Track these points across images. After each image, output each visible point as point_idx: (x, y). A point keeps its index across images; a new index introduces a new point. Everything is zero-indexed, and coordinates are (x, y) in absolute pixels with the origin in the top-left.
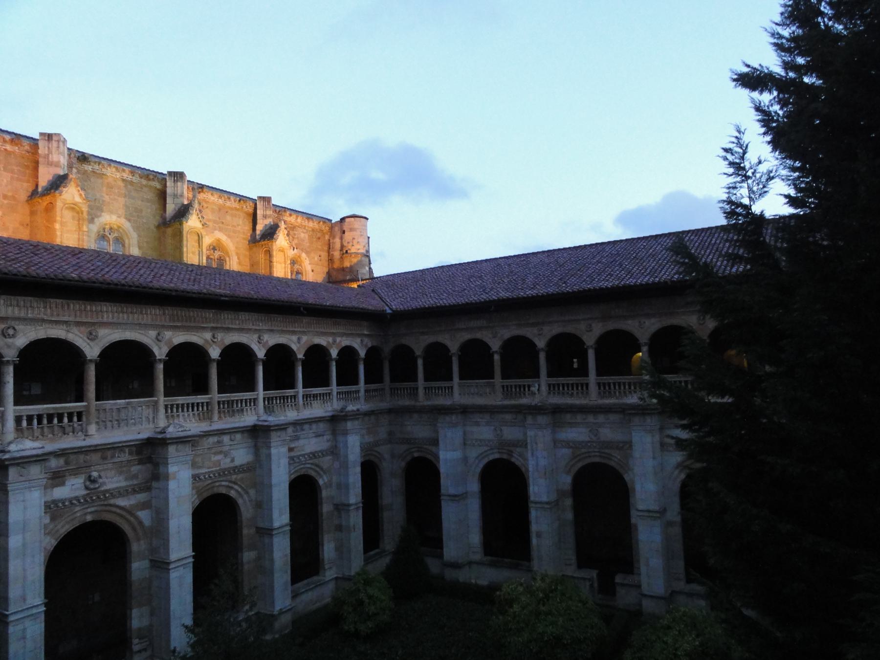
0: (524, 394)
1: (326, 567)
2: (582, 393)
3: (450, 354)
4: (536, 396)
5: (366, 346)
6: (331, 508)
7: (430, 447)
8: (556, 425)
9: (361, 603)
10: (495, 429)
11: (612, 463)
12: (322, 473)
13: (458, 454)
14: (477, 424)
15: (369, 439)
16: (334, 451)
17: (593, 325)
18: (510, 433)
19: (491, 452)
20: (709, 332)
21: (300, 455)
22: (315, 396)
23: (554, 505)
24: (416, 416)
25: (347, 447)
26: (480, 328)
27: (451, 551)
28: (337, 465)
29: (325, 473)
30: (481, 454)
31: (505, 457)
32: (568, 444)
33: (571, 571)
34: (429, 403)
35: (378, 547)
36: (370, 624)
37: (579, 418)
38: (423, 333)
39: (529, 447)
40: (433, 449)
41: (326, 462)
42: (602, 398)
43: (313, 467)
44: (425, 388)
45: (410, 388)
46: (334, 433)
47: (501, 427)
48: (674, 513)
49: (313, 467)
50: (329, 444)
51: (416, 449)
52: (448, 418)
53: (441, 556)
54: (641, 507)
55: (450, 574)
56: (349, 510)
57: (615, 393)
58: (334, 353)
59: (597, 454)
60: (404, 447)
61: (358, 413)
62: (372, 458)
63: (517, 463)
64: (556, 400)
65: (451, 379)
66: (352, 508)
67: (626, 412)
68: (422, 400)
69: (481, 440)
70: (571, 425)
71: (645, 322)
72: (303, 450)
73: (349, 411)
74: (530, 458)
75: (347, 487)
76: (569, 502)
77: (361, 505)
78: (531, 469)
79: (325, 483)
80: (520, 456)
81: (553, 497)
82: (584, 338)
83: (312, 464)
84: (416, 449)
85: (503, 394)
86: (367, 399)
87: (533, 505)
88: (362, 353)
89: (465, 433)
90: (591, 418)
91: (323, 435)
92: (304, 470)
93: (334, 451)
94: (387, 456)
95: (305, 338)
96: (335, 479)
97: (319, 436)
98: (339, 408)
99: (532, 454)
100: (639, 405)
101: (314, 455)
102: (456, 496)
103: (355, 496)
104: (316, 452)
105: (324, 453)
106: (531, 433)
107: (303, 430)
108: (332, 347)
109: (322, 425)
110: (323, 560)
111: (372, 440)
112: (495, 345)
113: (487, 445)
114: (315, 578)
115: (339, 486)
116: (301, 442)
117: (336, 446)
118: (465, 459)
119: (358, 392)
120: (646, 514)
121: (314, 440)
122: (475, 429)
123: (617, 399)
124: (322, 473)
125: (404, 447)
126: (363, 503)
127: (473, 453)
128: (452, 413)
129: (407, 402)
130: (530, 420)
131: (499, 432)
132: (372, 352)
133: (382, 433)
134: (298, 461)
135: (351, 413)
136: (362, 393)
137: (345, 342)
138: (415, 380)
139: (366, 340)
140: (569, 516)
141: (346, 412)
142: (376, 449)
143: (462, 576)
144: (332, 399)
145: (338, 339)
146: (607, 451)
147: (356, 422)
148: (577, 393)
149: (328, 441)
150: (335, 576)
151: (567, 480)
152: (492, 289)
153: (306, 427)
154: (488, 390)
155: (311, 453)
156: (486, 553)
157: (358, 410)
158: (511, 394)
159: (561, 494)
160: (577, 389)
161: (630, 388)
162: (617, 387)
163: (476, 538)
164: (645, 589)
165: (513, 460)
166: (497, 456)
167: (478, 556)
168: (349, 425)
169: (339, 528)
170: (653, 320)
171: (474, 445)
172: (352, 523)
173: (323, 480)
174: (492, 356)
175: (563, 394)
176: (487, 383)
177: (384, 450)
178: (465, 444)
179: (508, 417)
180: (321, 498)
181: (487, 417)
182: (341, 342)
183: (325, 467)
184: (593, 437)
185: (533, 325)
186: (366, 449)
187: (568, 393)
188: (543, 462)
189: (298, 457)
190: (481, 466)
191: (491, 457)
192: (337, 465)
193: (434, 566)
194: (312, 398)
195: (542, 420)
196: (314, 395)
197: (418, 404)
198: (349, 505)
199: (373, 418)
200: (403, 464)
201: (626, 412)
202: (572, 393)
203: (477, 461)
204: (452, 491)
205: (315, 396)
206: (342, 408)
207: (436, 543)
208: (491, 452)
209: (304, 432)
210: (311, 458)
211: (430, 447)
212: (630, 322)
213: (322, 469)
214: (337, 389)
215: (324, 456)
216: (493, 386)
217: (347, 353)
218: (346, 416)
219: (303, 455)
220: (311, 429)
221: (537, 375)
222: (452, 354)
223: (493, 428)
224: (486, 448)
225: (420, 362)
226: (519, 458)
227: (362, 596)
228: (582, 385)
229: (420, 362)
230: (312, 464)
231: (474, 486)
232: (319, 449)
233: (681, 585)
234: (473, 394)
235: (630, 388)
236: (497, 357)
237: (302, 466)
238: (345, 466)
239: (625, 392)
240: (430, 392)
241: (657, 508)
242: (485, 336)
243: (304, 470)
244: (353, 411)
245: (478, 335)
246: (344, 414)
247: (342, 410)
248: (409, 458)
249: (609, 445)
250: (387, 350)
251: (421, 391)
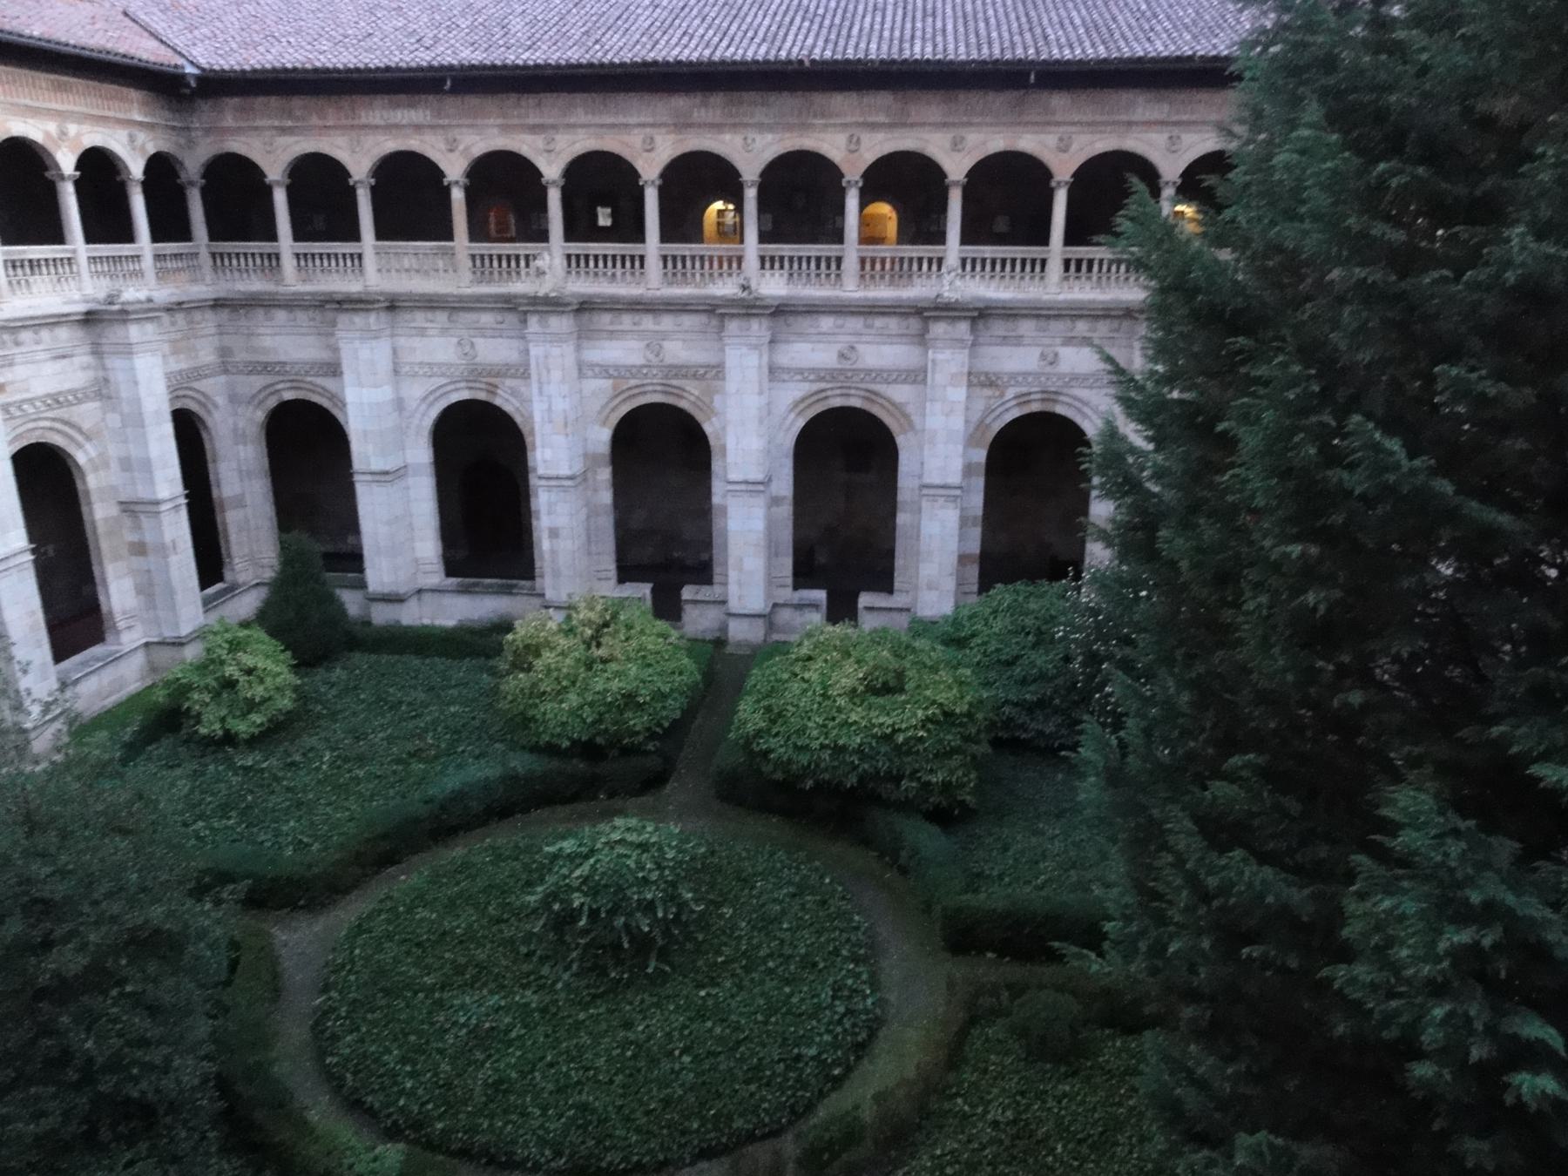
0: (518, 273)
1: (121, 625)
2: (633, 274)
3: (351, 183)
4: (547, 277)
5: (143, 148)
6: (114, 511)
7: (319, 381)
8: (584, 335)
9: (230, 684)
10: (459, 343)
11: (683, 404)
12: (79, 438)
13: (385, 393)
14: (422, 332)
15: (180, 364)
16: (102, 390)
17: (659, 139)
18: (495, 350)
19: (452, 387)
20: (863, 167)
21: (24, 401)
22: (34, 265)
23: (580, 480)
24: (281, 316)
25: (136, 383)
26: (418, 128)
27: (380, 572)
28: (114, 420)
29: (88, 438)
30: (431, 393)
31: (482, 396)
32: (605, 371)
33: (610, 589)
34: (308, 288)
35: (221, 579)
36: (257, 718)
37: (627, 320)
38: (283, 131)
39: (534, 376)
40: (329, 383)
41: (87, 414)
42: (670, 284)
43: (58, 426)
44: (297, 256)
45: (261, 255)
46: (97, 351)
47: (474, 340)
48: (784, 485)
49: (58, 426)
50: (91, 374)
51: (288, 385)
52: (358, 319)
53: (362, 585)
54: (733, 476)
55: (381, 615)
56: (159, 513)
57: (693, 275)
58: (67, 162)
59: (659, 388)
60: (258, 381)
61: (151, 305)
62: (193, 406)
63: (507, 408)
64: (582, 286)
65: (354, 235)
66: (163, 507)
67: (716, 311)
68: (292, 279)
69: (430, 365)
70: (612, 335)
71: (754, 140)
72: (27, 390)
73: (129, 303)
74: (536, 398)
75: (147, 465)
76: (605, 474)
77: (184, 501)
78: (537, 417)
79: (91, 460)
80: (512, 394)
81: (578, 468)
82: (640, 165)
83: (53, 420)
84: (288, 385)
85: (474, 273)
86: (162, 275)
87: (543, 482)
88: (136, 168)
89: (395, 351)
90: (648, 322)
91: (72, 356)
92: (38, 433)
93: (102, 390)
94: (220, 400)
96: (114, 451)
97: (64, 357)
98: (102, 295)
99: (541, 392)
100: (743, 300)
101: (56, 400)
102: (386, 473)
103: (168, 481)
104: (60, 393)
105: (80, 396)
106: (536, 351)
107: (17, 344)
108: (59, 147)
109: (63, 333)
110: (110, 613)
111: (184, 366)
112: (454, 169)
113: (443, 375)
114: (96, 650)
115: (126, 464)
116: (20, 372)
117: (106, 380)
118: (399, 404)
119: (137, 258)
120: (743, 487)
121: (50, 368)
122: (417, 342)
123: (697, 286)
124: (79, 438)
125: (258, 381)
126: (187, 496)
127: (415, 391)
128: (368, 310)
129: (255, 284)
130: (534, 323)
131: (467, 349)
132: (161, 169)
133: (207, 355)
134: (18, 413)
135: (138, 306)
136: (148, 262)
137: (94, 137)
138: (272, 236)
139: (142, 137)
140: (606, 497)
141: (123, 303)
142: (196, 385)
143: (412, 615)
144: (79, 273)
145: (72, 129)
146: (674, 382)
147: (150, 327)
148: (624, 274)
149: (85, 368)
150: (144, 641)
151: (602, 437)
152: (436, 40)
153: (26, 336)
154: (440, 264)
155: (48, 395)
156: (450, 571)
157: (150, 300)
158: (491, 273)
159: (591, 459)
160: (623, 266)
161: (721, 267)
162: (698, 265)
163: (428, 547)
164: (734, 605)
165: (498, 402)
166: (465, 395)
167: (435, 575)
168: (134, 332)
169: (139, 549)
170: (769, 137)
171: (415, 375)
172: (168, 538)
173: (85, 452)
174: (446, 191)
175: (596, 274)
176: (439, 248)
177: (215, 387)
178: (396, 372)
179: (487, 319)
180: (87, 492)
181: (441, 317)
182: (79, 135)
183: (86, 426)
184: (651, 357)
185: (535, 129)
186: (178, 384)
187: (605, 274)
188: (560, 405)
189: (19, 405)
190: (434, 413)
191: (455, 397)
192: (114, 420)
193: (351, 601)
194: (28, 270)
195: (561, 324)
196: (30, 261)
197: (281, 289)
198: (157, 503)
199: (180, 318)
200: (260, 416)
201: (716, 311)
202: (614, 275)
203: (424, 407)
204: (377, 464)
205: (34, 265)
206: (110, 296)
207: (352, 561)
208: (452, 387)
209: (24, 349)
211: (319, 381)
212: (728, 137)
213: (80, 430)
214: (87, 250)
215: (80, 402)
216: (451, 254)
217: (97, 165)
218: (124, 312)
219: (31, 401)
220: (37, 343)
221: (542, 236)
222: (356, 182)
223: (455, 340)
224: (444, 381)
225: (280, 198)
226: (511, 398)
227: (231, 671)
228: (632, 258)
229: (280, 198)
230: (53, 420)
231: (421, 454)
232: (67, 386)
233: (787, 594)
234: (407, 270)
235: (721, 267)
236: (458, 195)
237: (31, 425)
238: (135, 421)
239: (711, 275)
240: (310, 264)
241: (760, 477)
242: (431, 146)
243: (38, 433)
244: (139, 302)
245: (414, 144)
246: (116, 307)
247: (110, 300)
248: (272, 403)
249: (680, 371)
250: (193, 164)
251: (288, 263)
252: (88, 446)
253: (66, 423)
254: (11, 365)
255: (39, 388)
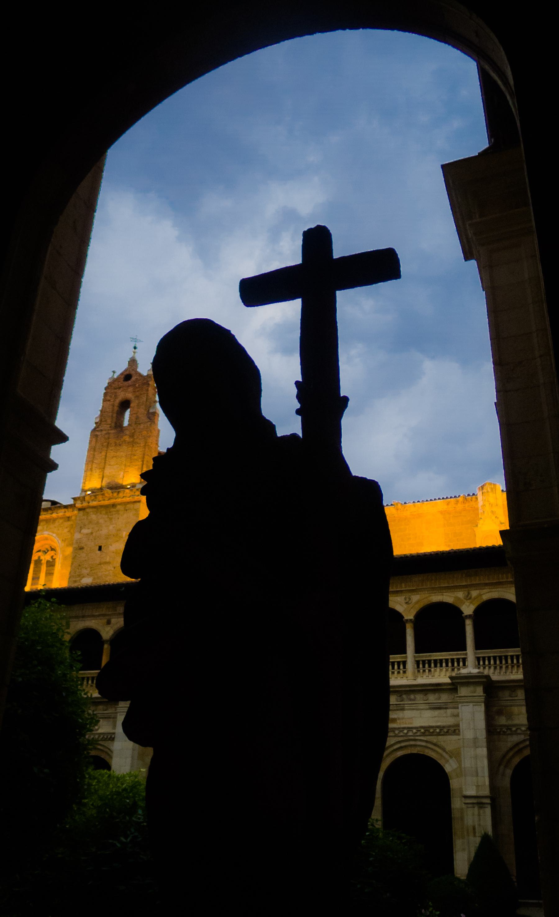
29: (451, 757)
72: (411, 723)
91: (446, 708)
95: (415, 598)
121: (428, 714)
145: (474, 593)
183: (448, 748)
210: (423, 734)
213: (444, 750)
219: (410, 729)
252: (451, 761)
253: (435, 745)
254: (403, 709)
255: (418, 723)
